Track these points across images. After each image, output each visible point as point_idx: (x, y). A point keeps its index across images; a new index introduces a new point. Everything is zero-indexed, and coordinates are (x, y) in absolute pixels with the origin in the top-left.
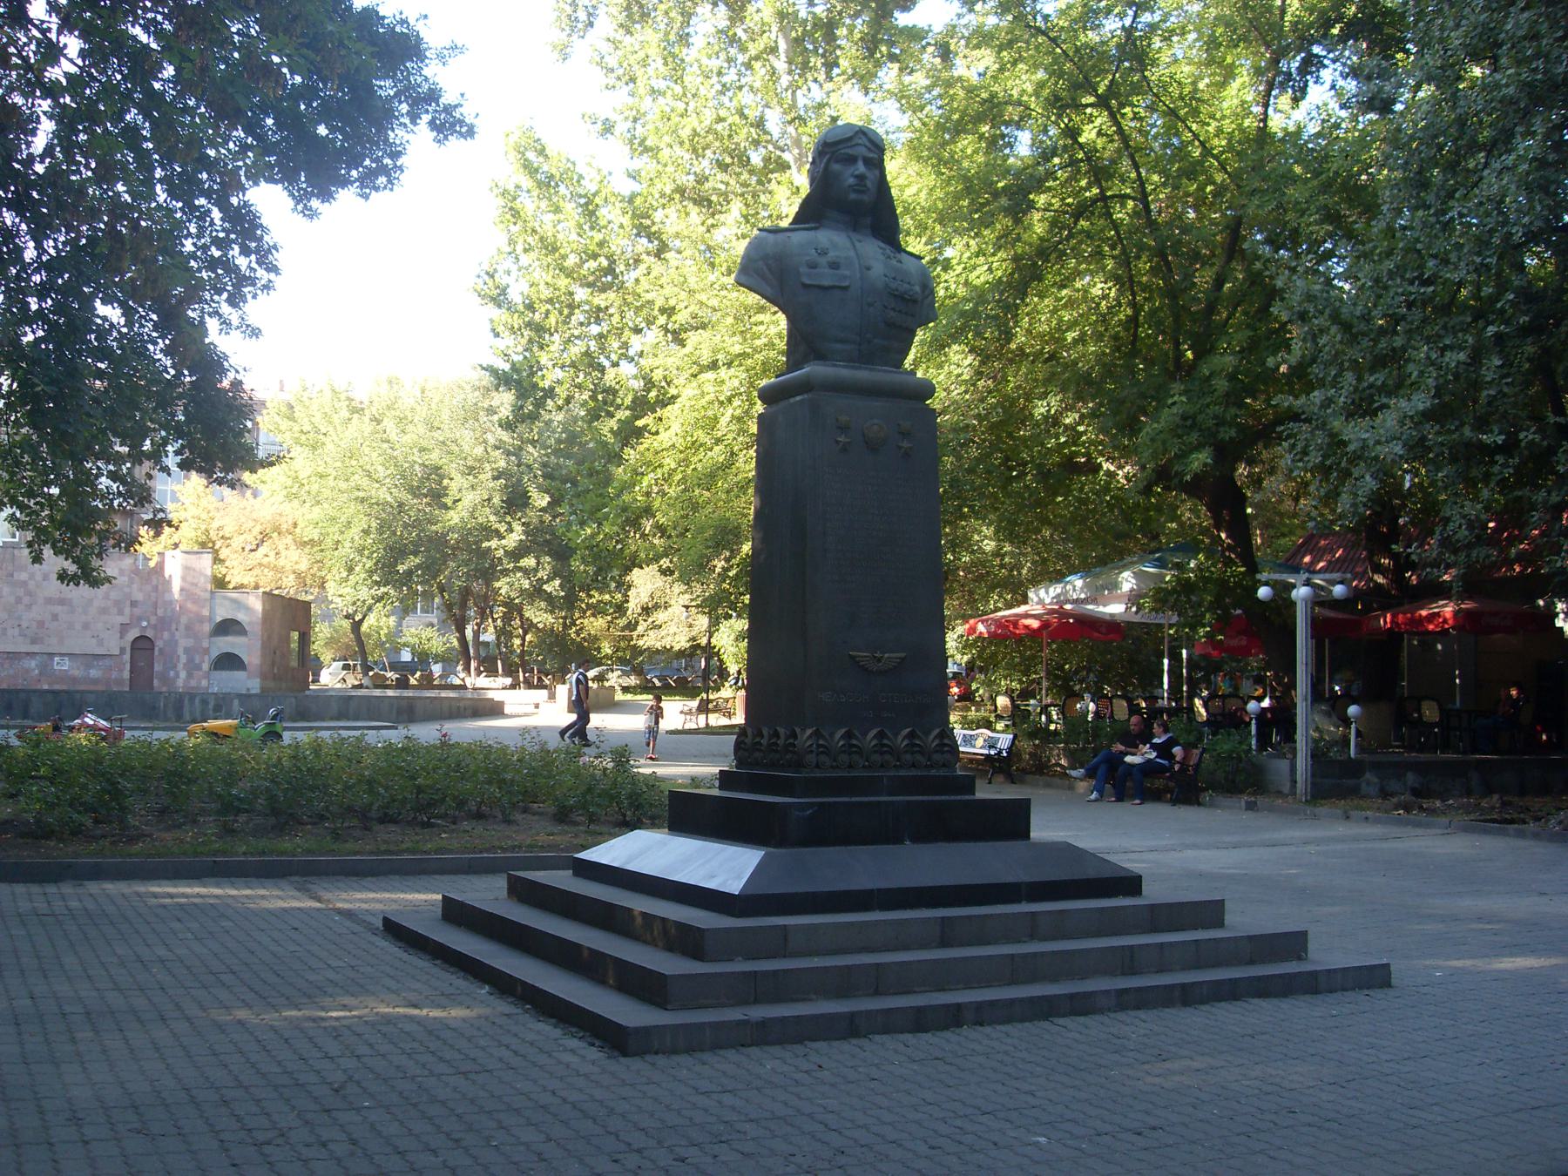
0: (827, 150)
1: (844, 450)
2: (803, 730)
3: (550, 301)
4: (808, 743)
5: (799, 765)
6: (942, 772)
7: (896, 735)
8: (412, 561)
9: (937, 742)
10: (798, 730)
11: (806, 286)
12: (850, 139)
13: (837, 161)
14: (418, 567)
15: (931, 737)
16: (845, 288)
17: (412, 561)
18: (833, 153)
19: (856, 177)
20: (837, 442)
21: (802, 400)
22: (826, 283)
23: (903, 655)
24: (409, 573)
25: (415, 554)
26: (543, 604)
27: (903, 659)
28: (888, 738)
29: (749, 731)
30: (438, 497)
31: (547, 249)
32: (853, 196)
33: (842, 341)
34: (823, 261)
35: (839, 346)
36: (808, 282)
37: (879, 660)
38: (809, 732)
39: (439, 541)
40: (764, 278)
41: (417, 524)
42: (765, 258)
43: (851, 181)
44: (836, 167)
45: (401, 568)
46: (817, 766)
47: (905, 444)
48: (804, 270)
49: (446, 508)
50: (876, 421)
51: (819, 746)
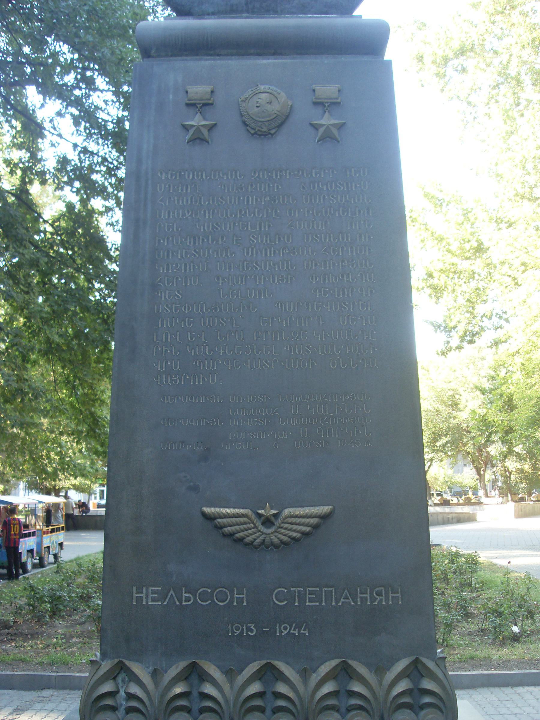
3: (441, 271)
4: (107, 687)
7: (305, 674)
8: (444, 440)
9: (403, 686)
14: (447, 443)
15: (390, 676)
17: (444, 440)
20: (186, 128)
23: (325, 509)
24: (444, 446)
25: (446, 436)
26: (515, 458)
27: (325, 517)
28: (286, 680)
30: (455, 405)
31: (437, 239)
37: (268, 522)
39: (458, 428)
41: (447, 420)
45: (438, 444)
47: (327, 120)
49: (460, 411)
50: (262, 88)
51: (131, 696)
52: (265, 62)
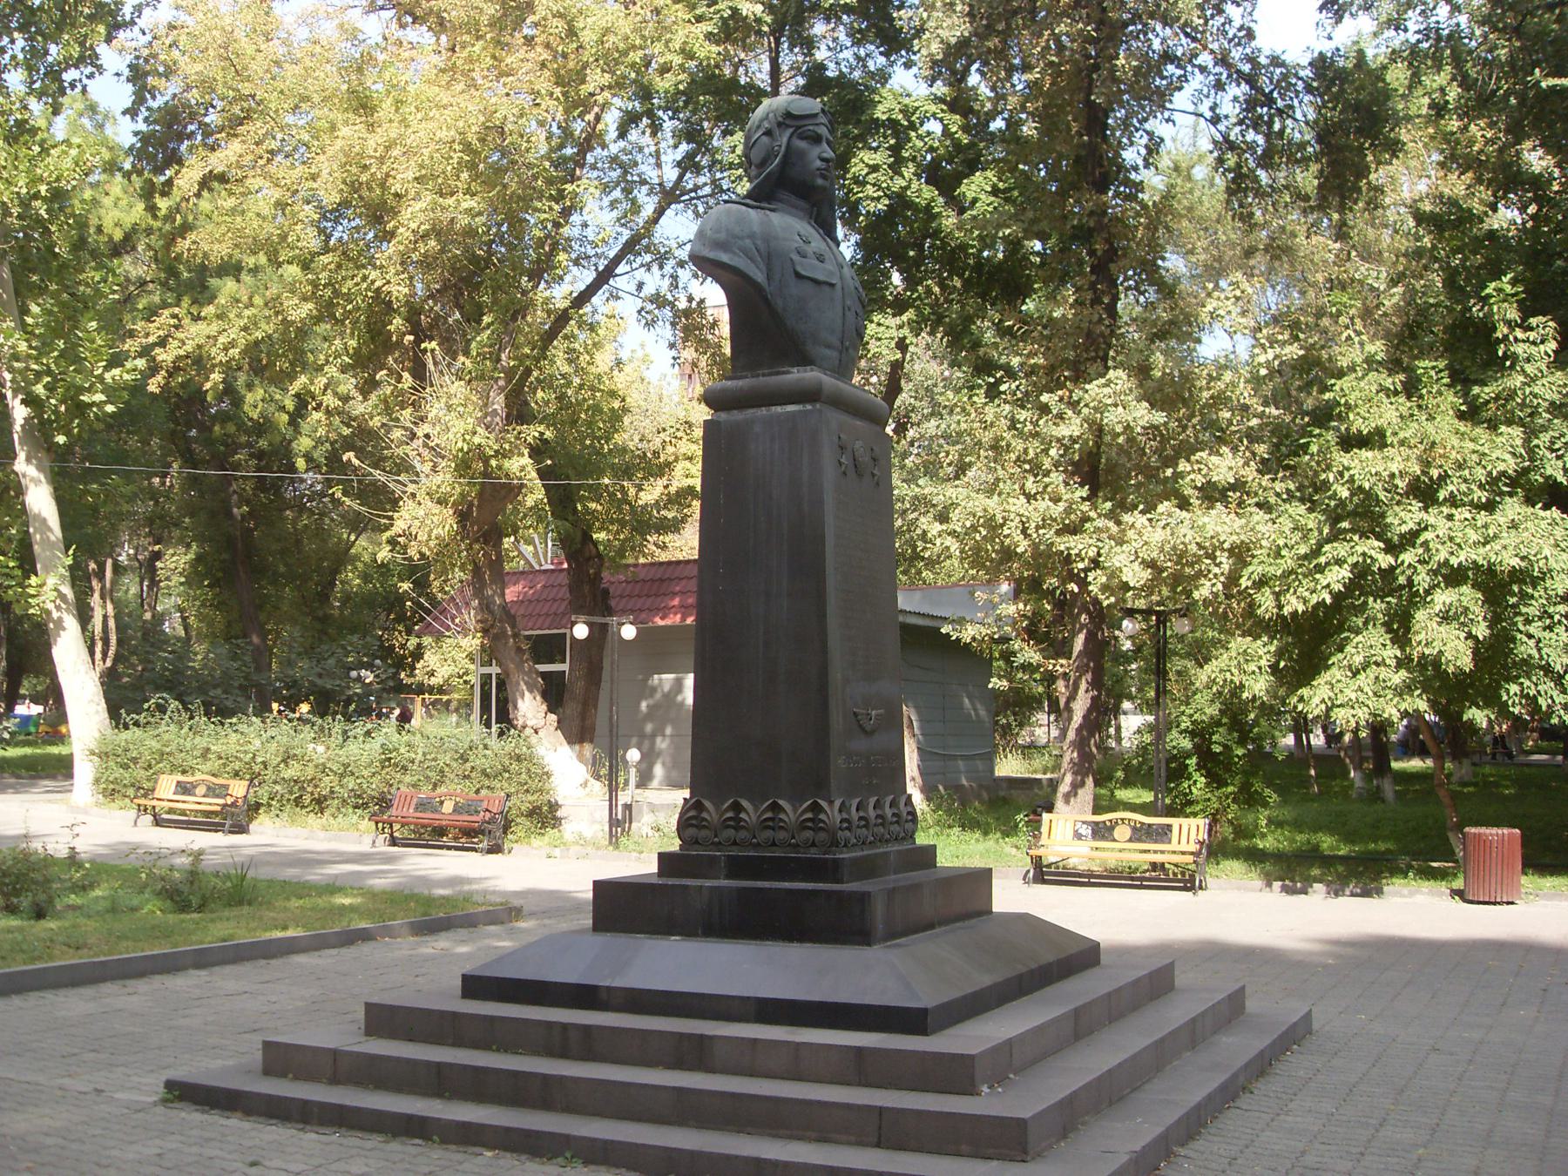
0: (787, 122)
1: (845, 473)
2: (831, 803)
5: (835, 843)
6: (906, 846)
10: (823, 804)
11: (798, 276)
12: (815, 115)
13: (802, 138)
16: (832, 285)
18: (800, 127)
19: (823, 160)
20: (840, 464)
21: (800, 411)
22: (821, 277)
29: (707, 804)
32: (820, 181)
33: (829, 346)
34: (809, 249)
35: (828, 352)
36: (803, 273)
38: (837, 803)
40: (751, 259)
42: (752, 236)
43: (818, 163)
44: (802, 144)
46: (845, 846)
48: (795, 257)
52: (858, 423)
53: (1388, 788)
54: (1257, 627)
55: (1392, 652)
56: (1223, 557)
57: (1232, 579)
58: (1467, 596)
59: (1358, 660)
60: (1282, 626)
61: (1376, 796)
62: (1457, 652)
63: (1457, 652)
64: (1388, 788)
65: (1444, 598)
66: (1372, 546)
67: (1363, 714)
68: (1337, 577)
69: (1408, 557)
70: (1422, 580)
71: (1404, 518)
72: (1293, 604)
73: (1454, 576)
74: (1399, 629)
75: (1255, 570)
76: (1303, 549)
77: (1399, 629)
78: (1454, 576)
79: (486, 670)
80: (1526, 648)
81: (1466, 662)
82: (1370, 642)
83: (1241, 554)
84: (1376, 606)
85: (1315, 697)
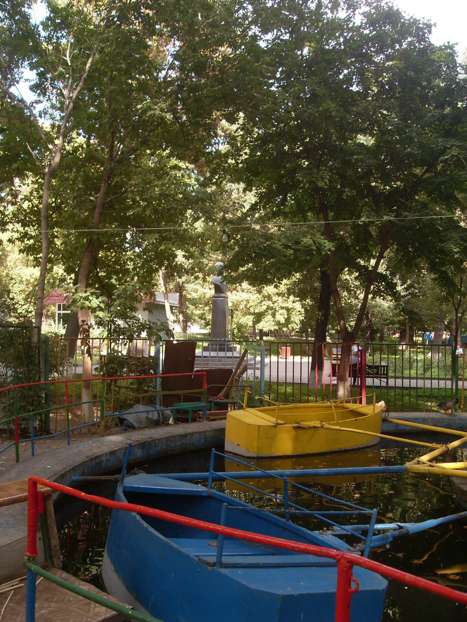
53: (262, 343)
54: (250, 314)
55: (272, 319)
56: (244, 301)
57: (246, 306)
58: (284, 311)
59: (267, 320)
60: (254, 314)
61: (260, 345)
62: (283, 321)
63: (283, 321)
64: (262, 343)
65: (281, 311)
66: (270, 303)
67: (268, 329)
68: (264, 307)
69: (276, 304)
70: (277, 309)
71: (275, 298)
72: (257, 311)
73: (282, 308)
74: (274, 315)
75: (250, 304)
76: (258, 301)
77: (274, 315)
78: (282, 308)
79: (59, 312)
80: (292, 319)
81: (284, 322)
82: (269, 317)
83: (248, 301)
84: (270, 312)
85: (259, 326)
